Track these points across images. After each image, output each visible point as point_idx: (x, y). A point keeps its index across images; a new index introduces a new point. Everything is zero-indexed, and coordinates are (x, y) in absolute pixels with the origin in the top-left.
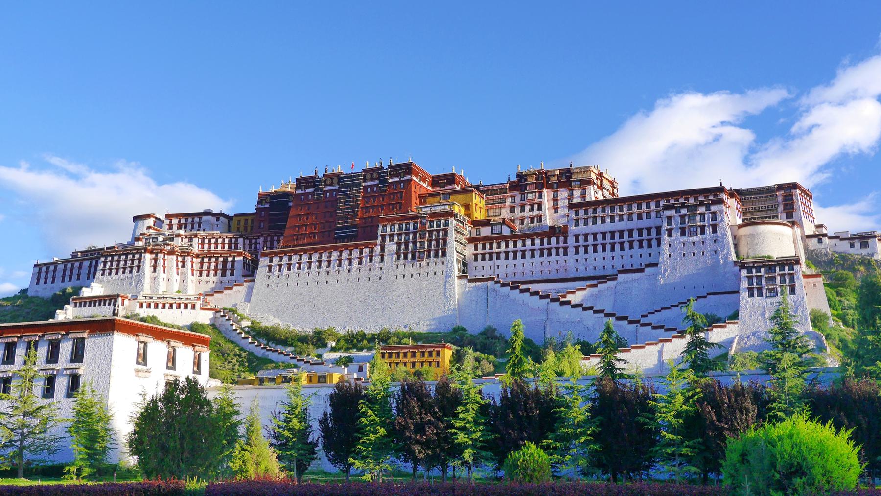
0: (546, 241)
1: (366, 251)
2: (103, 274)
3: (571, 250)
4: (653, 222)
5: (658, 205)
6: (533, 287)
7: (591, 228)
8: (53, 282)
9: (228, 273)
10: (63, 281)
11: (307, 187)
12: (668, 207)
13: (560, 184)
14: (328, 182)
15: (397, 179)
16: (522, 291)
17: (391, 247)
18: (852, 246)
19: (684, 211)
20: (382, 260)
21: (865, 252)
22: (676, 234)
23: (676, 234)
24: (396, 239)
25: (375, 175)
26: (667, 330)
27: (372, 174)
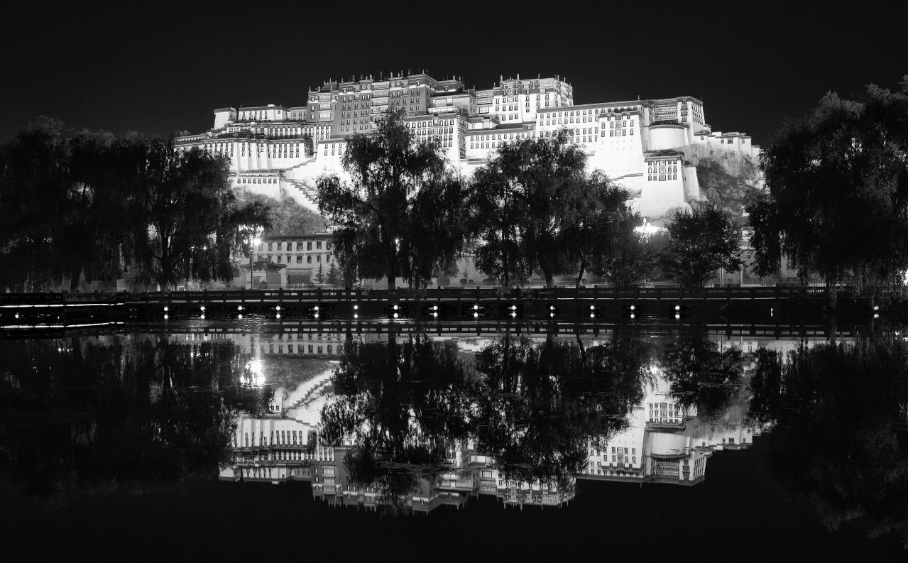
4: (593, 125)
5: (597, 112)
9: (295, 154)
12: (602, 116)
13: (531, 91)
14: (364, 87)
15: (414, 87)
18: (722, 142)
19: (613, 119)
21: (731, 145)
22: (607, 134)
23: (607, 134)
25: (398, 84)
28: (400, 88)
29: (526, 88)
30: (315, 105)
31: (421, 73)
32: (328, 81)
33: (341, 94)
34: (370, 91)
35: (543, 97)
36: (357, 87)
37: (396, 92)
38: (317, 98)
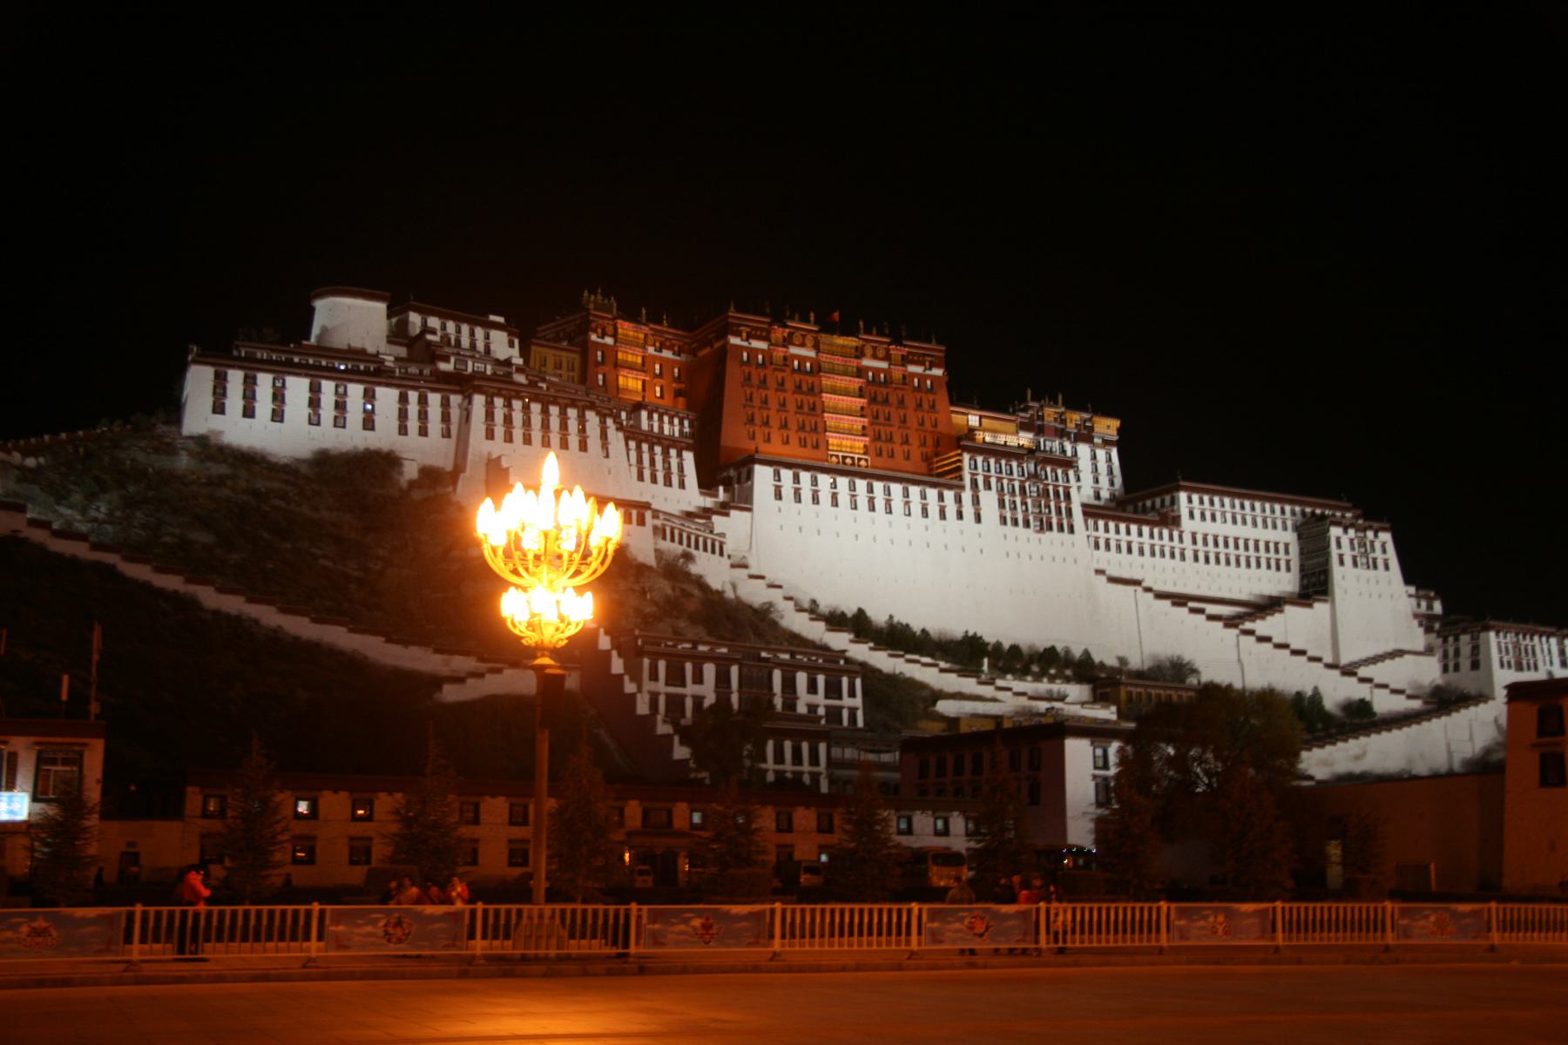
0: (1156, 531)
1: (949, 495)
2: (490, 435)
3: (1189, 554)
6: (1212, 609)
7: (1210, 528)
8: (278, 416)
10: (315, 420)
11: (749, 337)
14: (797, 338)
15: (918, 369)
16: (1193, 611)
17: (989, 499)
19: (1351, 532)
20: (978, 519)
22: (1348, 560)
23: (1348, 560)
24: (993, 481)
26: (1410, 697)
27: (874, 349)
28: (884, 365)
29: (1071, 427)
30: (604, 347)
31: (930, 342)
32: (593, 291)
33: (734, 340)
34: (812, 354)
35: (1101, 454)
36: (779, 333)
37: (877, 371)
38: (610, 329)
